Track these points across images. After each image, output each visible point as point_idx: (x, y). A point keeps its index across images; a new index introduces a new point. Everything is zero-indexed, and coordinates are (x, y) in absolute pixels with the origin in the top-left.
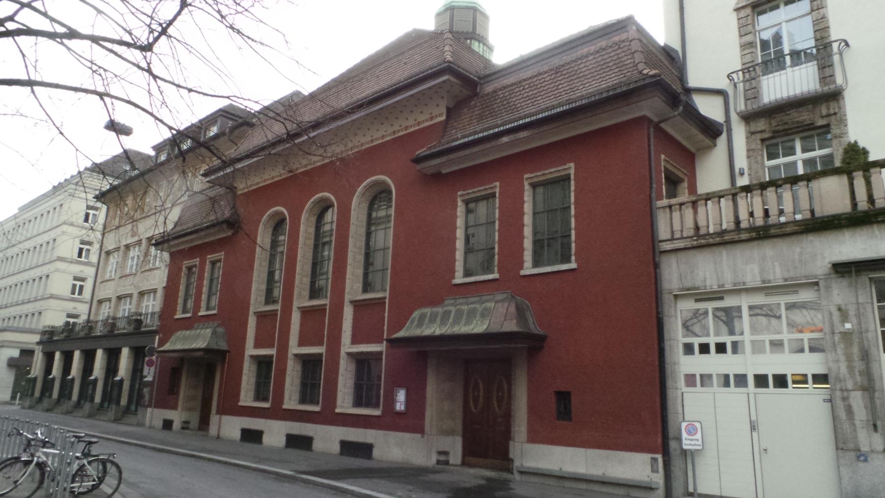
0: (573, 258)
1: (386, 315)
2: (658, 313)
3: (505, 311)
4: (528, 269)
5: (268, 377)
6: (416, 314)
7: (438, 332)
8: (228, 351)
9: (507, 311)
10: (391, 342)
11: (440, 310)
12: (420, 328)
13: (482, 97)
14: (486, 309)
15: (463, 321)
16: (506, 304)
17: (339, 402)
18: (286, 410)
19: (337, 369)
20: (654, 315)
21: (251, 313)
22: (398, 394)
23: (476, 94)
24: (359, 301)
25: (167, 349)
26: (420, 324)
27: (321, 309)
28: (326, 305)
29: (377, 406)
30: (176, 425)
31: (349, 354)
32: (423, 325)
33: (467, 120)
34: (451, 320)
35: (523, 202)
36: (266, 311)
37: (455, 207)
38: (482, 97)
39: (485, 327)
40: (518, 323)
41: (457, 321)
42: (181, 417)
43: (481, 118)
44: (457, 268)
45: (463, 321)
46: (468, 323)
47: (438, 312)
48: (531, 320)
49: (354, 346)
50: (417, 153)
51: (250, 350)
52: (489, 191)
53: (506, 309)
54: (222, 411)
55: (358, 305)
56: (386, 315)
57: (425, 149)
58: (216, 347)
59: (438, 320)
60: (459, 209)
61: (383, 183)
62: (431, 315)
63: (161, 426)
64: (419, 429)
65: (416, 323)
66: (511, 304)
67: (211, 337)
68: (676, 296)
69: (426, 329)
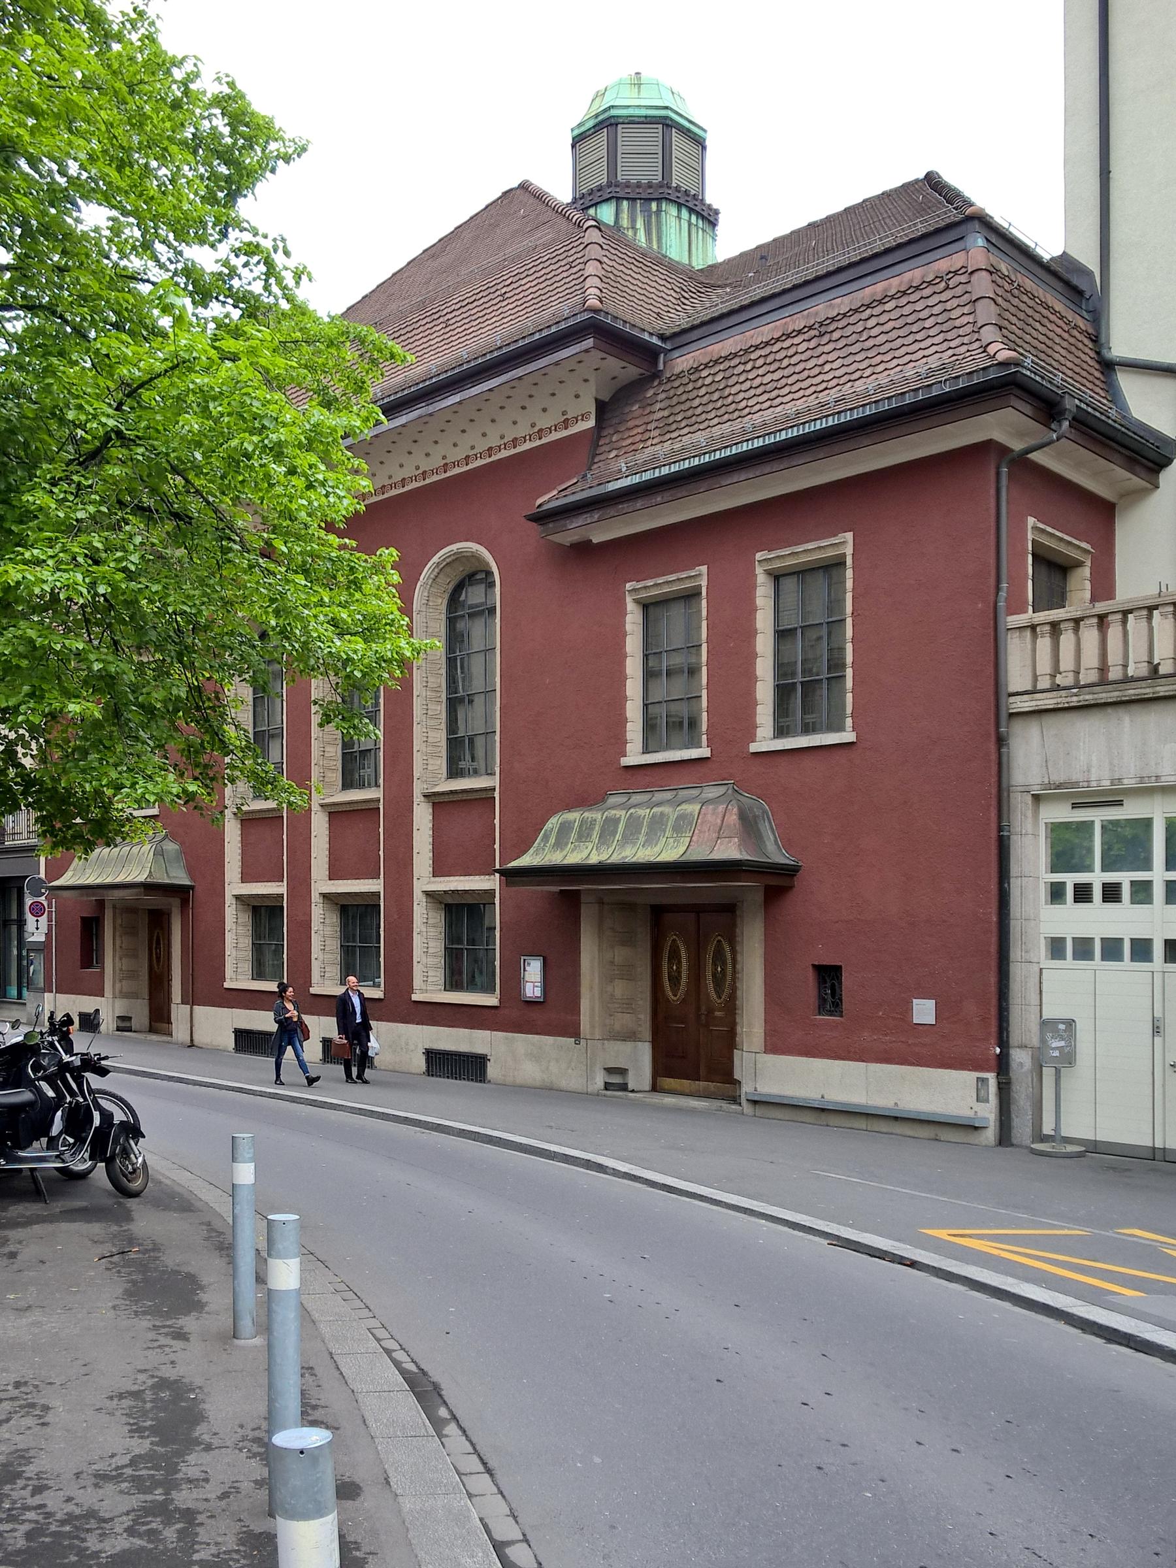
0: (849, 722)
1: (497, 821)
2: (1000, 829)
3: (719, 821)
4: (765, 740)
5: (276, 932)
6: (553, 822)
7: (594, 859)
8: (192, 887)
9: (723, 821)
10: (511, 876)
11: (596, 816)
12: (562, 850)
13: (669, 380)
14: (682, 817)
15: (642, 838)
16: (721, 808)
17: (417, 982)
18: (415, 1002)
20: (994, 834)
21: (418, 798)
22: (527, 968)
23: (657, 375)
24: (443, 793)
26: (559, 844)
27: (368, 811)
29: (490, 989)
30: (107, 1023)
32: (566, 844)
33: (640, 430)
35: (754, 610)
36: (357, 802)
38: (669, 380)
39: (682, 849)
40: (743, 844)
41: (627, 839)
42: (113, 1011)
43: (666, 428)
44: (760, 720)
45: (642, 838)
46: (649, 842)
47: (595, 820)
48: (772, 837)
49: (437, 879)
50: (539, 502)
51: (234, 886)
52: (831, 553)
53: (720, 816)
54: (192, 998)
55: (440, 803)
57: (555, 492)
59: (595, 835)
60: (760, 591)
61: (475, 557)
62: (581, 826)
63: (320, 1056)
64: (571, 1030)
65: (552, 840)
66: (730, 807)
68: (1037, 798)
69: (573, 851)
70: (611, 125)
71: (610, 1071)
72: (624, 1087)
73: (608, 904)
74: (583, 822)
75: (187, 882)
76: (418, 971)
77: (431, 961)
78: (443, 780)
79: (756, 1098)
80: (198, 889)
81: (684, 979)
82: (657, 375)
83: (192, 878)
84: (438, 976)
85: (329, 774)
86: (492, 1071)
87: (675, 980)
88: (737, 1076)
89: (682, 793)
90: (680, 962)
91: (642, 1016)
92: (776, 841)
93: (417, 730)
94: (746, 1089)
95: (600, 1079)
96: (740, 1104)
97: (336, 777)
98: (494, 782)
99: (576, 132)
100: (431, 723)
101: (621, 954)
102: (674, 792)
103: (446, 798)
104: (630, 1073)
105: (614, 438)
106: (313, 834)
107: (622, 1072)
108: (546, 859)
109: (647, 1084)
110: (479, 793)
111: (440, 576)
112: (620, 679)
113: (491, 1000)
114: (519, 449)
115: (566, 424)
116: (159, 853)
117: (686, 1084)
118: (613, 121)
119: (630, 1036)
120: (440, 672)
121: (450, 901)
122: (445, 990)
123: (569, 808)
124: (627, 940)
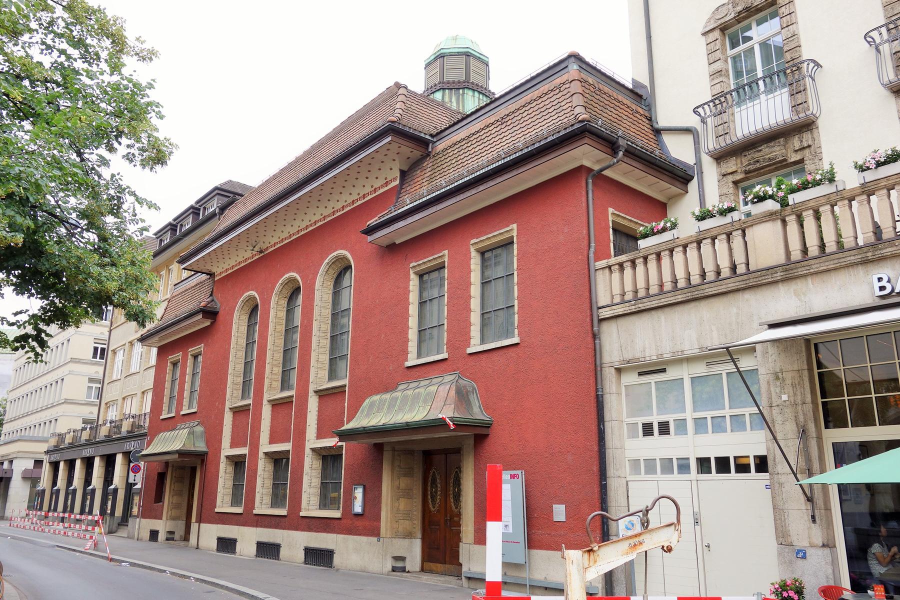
1: (346, 404)
12: (369, 418)
25: (148, 453)
30: (162, 536)
31: (313, 450)
37: (408, 279)
42: (165, 528)
49: (319, 441)
54: (200, 521)
55: (323, 394)
56: (346, 404)
67: (188, 438)
71: (397, 558)
72: (403, 570)
73: (398, 451)
74: (380, 400)
75: (205, 449)
80: (210, 454)
91: (415, 522)
95: (389, 564)
101: (404, 482)
104: (407, 560)
108: (360, 423)
112: (405, 316)
124: (408, 473)
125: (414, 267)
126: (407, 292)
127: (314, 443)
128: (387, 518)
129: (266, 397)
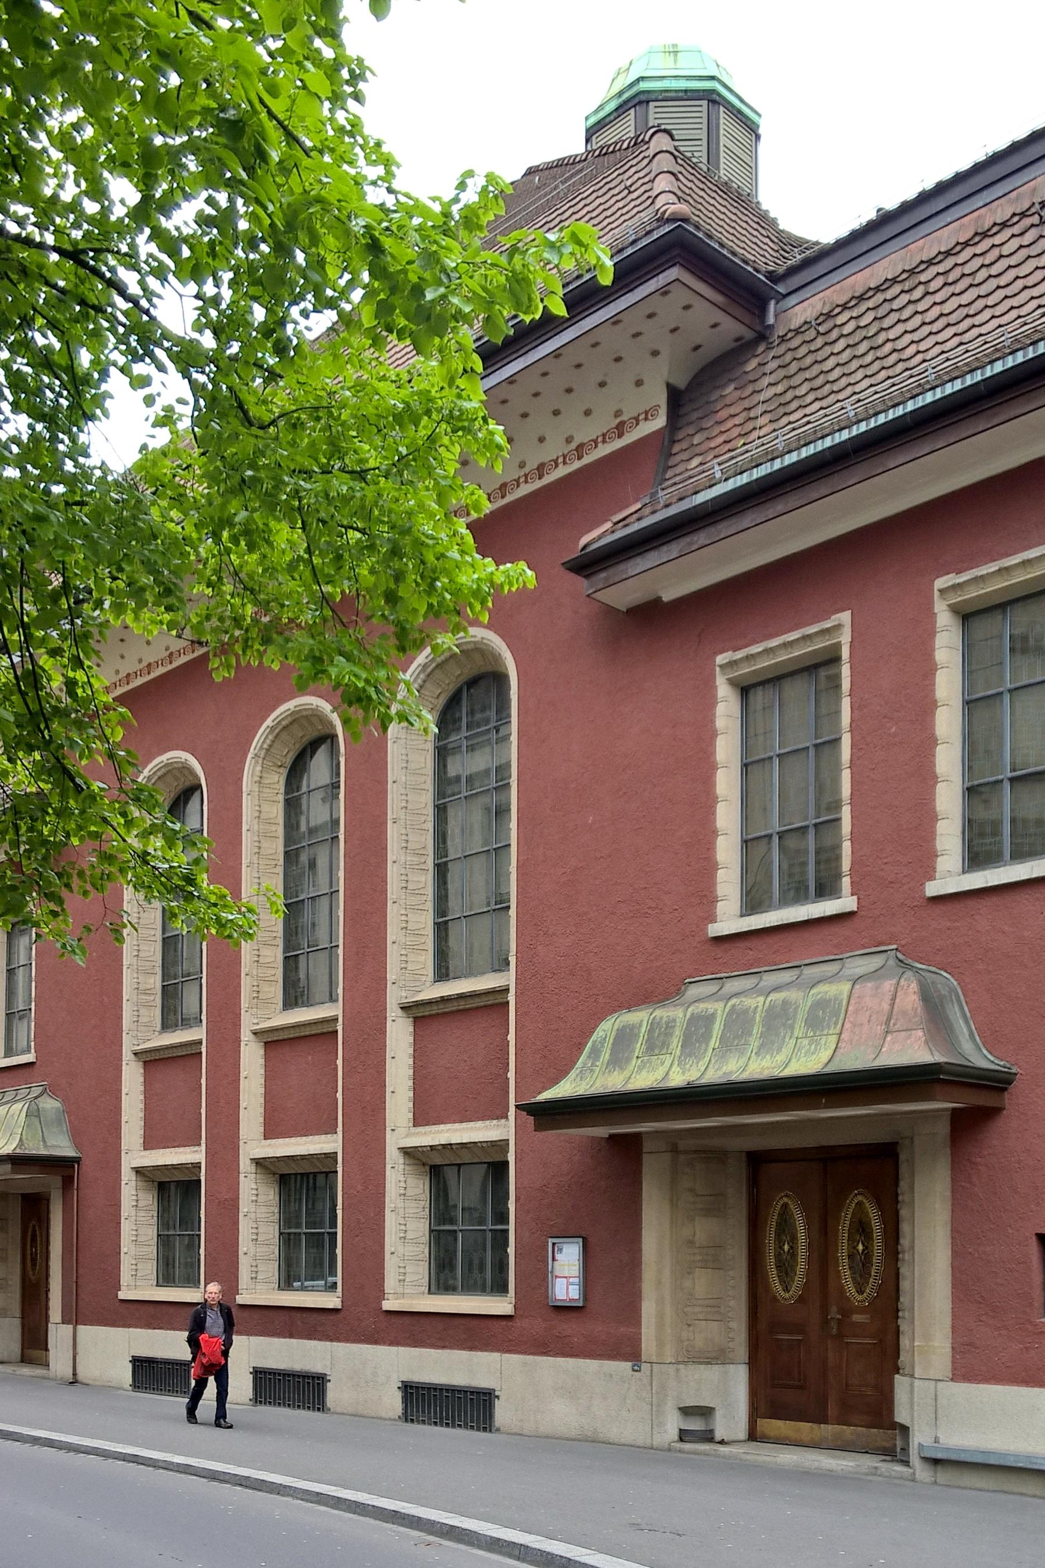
3: (886, 1006)
6: (606, 1029)
7: (677, 1079)
9: (892, 1005)
11: (675, 1013)
12: (622, 1069)
13: (783, 339)
14: (821, 1004)
15: (754, 1042)
16: (888, 985)
17: (391, 1283)
19: (117, 1205)
22: (558, 1256)
23: (762, 335)
24: (430, 1003)
26: (617, 1061)
28: (335, 1020)
29: (500, 1287)
32: (628, 1060)
33: (737, 421)
34: (714, 1042)
38: (783, 339)
39: (825, 1055)
41: (729, 1045)
43: (780, 408)
45: (754, 1042)
46: (767, 1046)
47: (674, 1021)
48: (965, 1030)
50: (584, 541)
53: (888, 998)
56: (511, 1037)
57: (608, 525)
58: (43, 1152)
59: (676, 1042)
62: (651, 1031)
65: (605, 1055)
66: (902, 982)
69: (640, 1069)
70: (640, 103)
71: (686, 1411)
72: (708, 1437)
73: (686, 1152)
74: (653, 1026)
76: (391, 1266)
77: (410, 1250)
78: (428, 984)
79: (939, 1456)
81: (801, 1267)
82: (762, 335)
83: (77, 1146)
84: (420, 1272)
85: (265, 988)
86: (502, 1413)
87: (786, 1269)
88: (901, 1416)
89: (808, 971)
90: (794, 1239)
91: (733, 1325)
92: (971, 1035)
93: (393, 913)
94: (920, 1438)
95: (673, 1424)
96: (906, 1463)
97: (276, 991)
98: (508, 979)
99: (593, 120)
100: (413, 900)
101: (703, 1229)
102: (796, 972)
103: (434, 1010)
104: (718, 1415)
105: (696, 440)
106: (243, 1075)
107: (705, 1412)
108: (598, 1084)
109: (741, 1431)
110: (484, 998)
111: (428, 685)
113: (501, 1305)
114: (548, 479)
115: (620, 430)
116: (34, 1114)
117: (805, 1429)
118: (643, 97)
119: (717, 1357)
120: (424, 826)
121: (438, 1161)
122: (430, 1292)
123: (630, 1006)
124: (714, 1208)
125: (732, 664)
126: (706, 735)
127: (408, 1135)
128: (660, 1316)
129: (249, 1022)
